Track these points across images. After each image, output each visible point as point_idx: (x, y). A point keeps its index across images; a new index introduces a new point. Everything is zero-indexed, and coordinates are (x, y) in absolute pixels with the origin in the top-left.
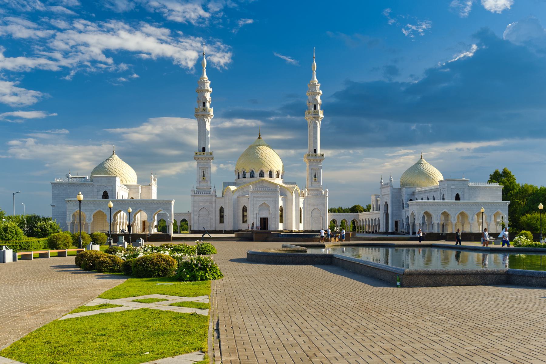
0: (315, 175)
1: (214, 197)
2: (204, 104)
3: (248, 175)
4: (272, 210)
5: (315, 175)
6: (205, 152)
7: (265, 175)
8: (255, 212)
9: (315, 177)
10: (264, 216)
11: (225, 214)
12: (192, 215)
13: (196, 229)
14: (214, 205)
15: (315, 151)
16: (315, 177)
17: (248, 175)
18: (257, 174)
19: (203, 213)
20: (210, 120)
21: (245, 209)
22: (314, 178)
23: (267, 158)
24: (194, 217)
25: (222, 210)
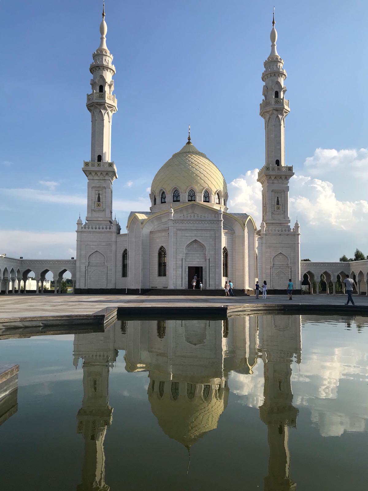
0: (278, 201)
1: (114, 235)
2: (102, 89)
3: (169, 197)
4: (209, 253)
5: (278, 201)
6: (101, 163)
7: (198, 199)
8: (180, 256)
9: (278, 203)
10: (195, 264)
11: (130, 262)
12: (78, 264)
13: (82, 287)
14: (113, 247)
15: (278, 162)
16: (278, 203)
17: (169, 197)
18: (184, 197)
19: (94, 260)
20: (111, 114)
21: (162, 253)
22: (276, 206)
23: (201, 170)
24: (81, 267)
25: (125, 254)
